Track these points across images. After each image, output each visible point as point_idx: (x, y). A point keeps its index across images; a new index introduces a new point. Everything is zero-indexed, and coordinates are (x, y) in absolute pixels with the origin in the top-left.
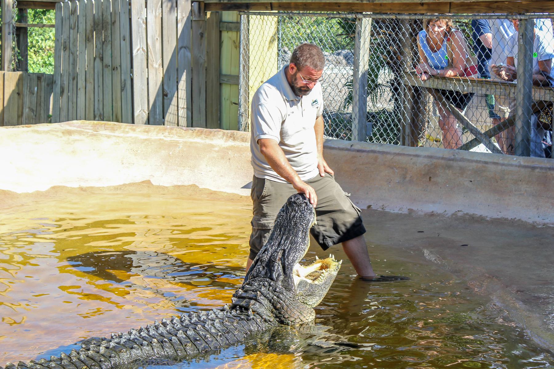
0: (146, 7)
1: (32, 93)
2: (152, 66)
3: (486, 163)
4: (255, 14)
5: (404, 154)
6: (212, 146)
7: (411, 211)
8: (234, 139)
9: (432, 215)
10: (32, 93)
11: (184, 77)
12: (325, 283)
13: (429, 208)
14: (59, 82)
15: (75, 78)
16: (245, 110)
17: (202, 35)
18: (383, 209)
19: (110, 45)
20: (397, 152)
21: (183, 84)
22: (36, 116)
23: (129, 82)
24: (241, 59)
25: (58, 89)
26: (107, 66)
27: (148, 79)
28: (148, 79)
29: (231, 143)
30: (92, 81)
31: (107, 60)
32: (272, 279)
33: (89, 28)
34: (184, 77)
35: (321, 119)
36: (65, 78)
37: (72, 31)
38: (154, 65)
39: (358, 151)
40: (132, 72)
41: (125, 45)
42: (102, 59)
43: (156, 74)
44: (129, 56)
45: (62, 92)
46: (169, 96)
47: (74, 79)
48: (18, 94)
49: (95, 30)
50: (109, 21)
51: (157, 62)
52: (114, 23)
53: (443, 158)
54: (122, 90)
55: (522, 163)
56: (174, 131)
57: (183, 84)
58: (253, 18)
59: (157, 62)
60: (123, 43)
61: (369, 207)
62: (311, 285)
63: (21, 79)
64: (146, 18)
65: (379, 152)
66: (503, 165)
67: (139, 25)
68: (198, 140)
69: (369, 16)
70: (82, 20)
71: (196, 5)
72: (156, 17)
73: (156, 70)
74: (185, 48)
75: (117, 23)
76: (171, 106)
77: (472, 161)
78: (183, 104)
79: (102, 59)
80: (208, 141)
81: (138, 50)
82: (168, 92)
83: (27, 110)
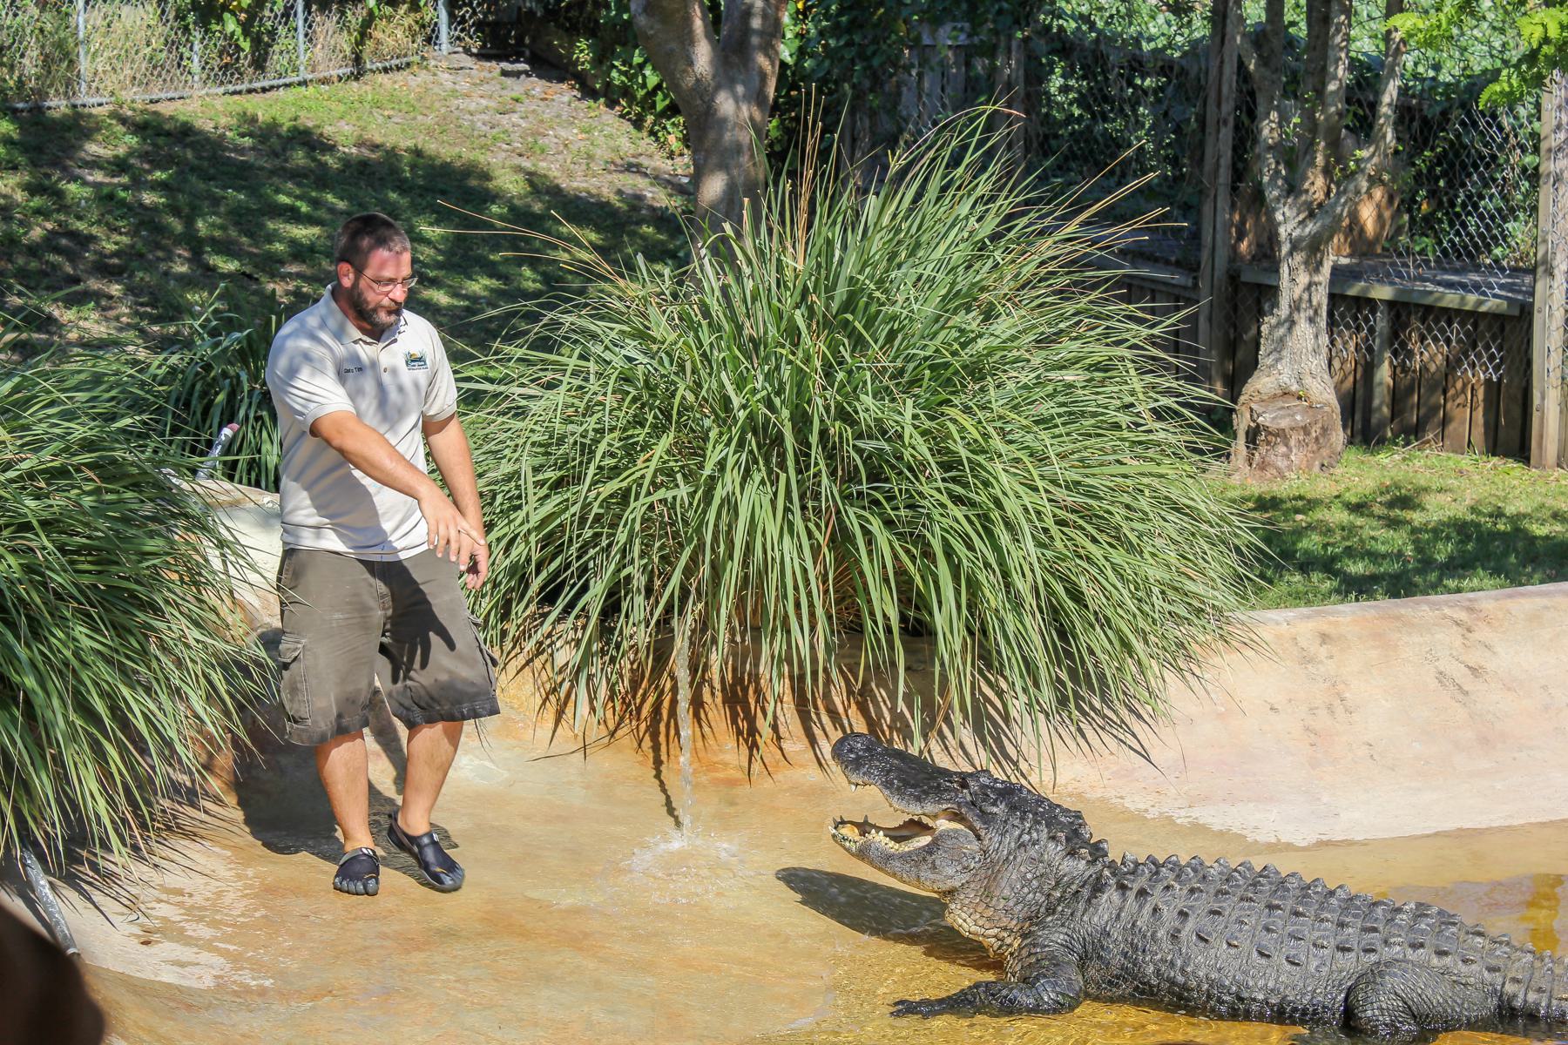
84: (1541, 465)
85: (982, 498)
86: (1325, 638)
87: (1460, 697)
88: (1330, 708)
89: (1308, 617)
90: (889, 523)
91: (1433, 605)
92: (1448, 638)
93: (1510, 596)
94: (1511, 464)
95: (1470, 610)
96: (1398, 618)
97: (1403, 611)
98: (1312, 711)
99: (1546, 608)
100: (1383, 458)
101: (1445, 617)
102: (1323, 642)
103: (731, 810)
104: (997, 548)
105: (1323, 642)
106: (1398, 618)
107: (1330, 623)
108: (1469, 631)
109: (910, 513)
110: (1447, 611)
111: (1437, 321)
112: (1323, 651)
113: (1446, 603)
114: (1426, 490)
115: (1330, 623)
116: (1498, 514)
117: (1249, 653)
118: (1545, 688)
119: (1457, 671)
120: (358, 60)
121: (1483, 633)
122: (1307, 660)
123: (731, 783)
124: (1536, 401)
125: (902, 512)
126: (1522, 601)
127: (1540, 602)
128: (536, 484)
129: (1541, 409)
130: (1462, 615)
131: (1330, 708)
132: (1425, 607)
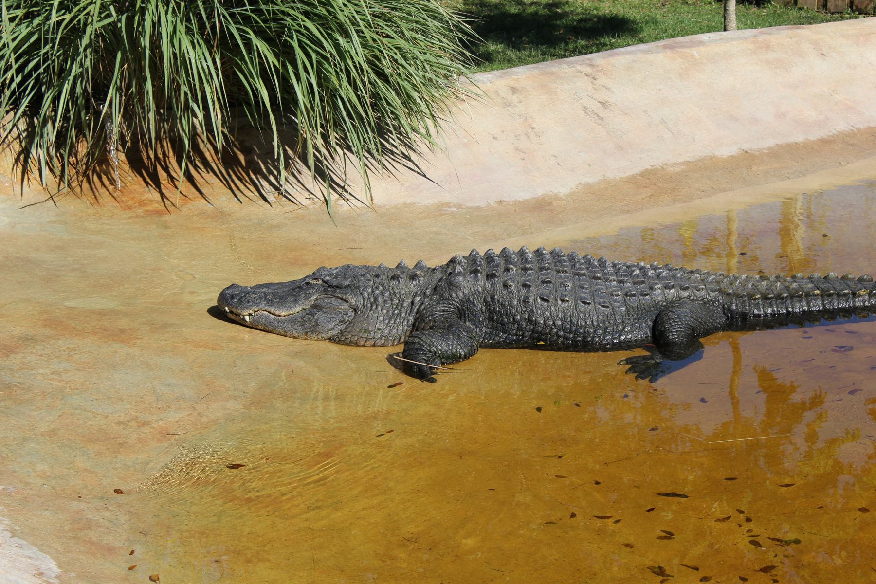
85: (322, 11)
86: (514, 90)
87: (599, 122)
88: (526, 134)
89: (501, 77)
90: (260, 33)
91: (569, 64)
92: (583, 84)
93: (611, 56)
95: (592, 66)
96: (552, 74)
97: (553, 69)
98: (517, 137)
99: (634, 61)
101: (579, 72)
102: (514, 93)
103: (169, 232)
104: (337, 46)
105: (514, 93)
106: (552, 74)
107: (514, 80)
108: (595, 79)
109: (276, 25)
110: (579, 67)
112: (515, 98)
113: (576, 62)
115: (514, 80)
117: (474, 103)
118: (645, 111)
119: (595, 106)
121: (602, 80)
122: (508, 105)
123: (159, 213)
125: (272, 25)
126: (619, 58)
127: (629, 58)
128: (12, 20)
130: (588, 70)
131: (526, 134)
132: (565, 66)
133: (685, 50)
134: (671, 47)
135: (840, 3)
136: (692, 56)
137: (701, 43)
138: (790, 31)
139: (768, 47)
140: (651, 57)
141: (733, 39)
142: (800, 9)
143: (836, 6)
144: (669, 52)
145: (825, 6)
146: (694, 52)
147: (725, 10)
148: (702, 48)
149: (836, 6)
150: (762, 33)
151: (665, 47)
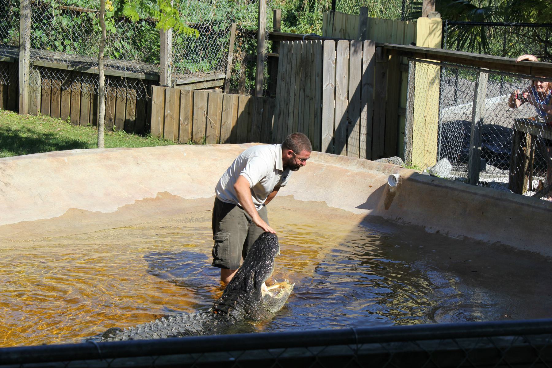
0: (336, 50)
1: (259, 113)
2: (339, 99)
3: (522, 204)
4: (420, 61)
5: (466, 192)
6: (347, 171)
7: (466, 238)
8: (364, 167)
9: (479, 243)
10: (259, 113)
11: (365, 109)
12: (283, 298)
13: (479, 237)
14: (278, 106)
15: (288, 104)
16: (409, 139)
17: (384, 74)
18: (447, 234)
19: (309, 80)
20: (462, 189)
21: (364, 114)
22: (261, 132)
23: (319, 111)
24: (408, 96)
25: (277, 112)
26: (307, 96)
27: (335, 109)
28: (335, 109)
29: (362, 170)
30: (298, 107)
31: (308, 91)
32: (246, 291)
33: (298, 64)
34: (365, 109)
35: (376, 163)
36: (282, 103)
37: (288, 65)
38: (341, 98)
39: (436, 186)
40: (322, 103)
41: (318, 79)
42: (304, 91)
43: (342, 105)
44: (320, 89)
45: (280, 114)
46: (352, 123)
47: (287, 104)
48: (249, 113)
49: (301, 66)
50: (310, 60)
51: (343, 96)
52: (312, 62)
53: (493, 198)
54: (315, 117)
55: (547, 207)
56: (323, 157)
57: (364, 114)
58: (417, 64)
59: (343, 96)
60: (317, 78)
61: (438, 232)
62: (273, 298)
63: (250, 101)
64: (336, 59)
65: (450, 188)
66: (534, 207)
67: (329, 65)
68: (338, 165)
69: (486, 71)
70: (294, 57)
71: (379, 49)
72: (344, 58)
73: (342, 102)
74: (368, 84)
75: (315, 62)
76: (353, 132)
77: (512, 202)
78: (364, 130)
79: (304, 91)
80: (345, 167)
81: (328, 85)
82: (352, 120)
83: (255, 127)
84: (23, 114)
93: (18, 159)
94: (12, 113)
95: (4, 164)
100: (365, 169)
108: (4, 171)
111: (76, 77)
114: (289, 166)
116: (9, 130)
118: (30, 189)
120: (455, 100)
121: (8, 171)
124: (21, 92)
129: (22, 94)
133: (60, 158)
134: (53, 156)
135: (186, 138)
136: (64, 161)
137: (71, 154)
138: (123, 151)
139: (108, 158)
140: (40, 160)
141: (89, 153)
142: (166, 140)
143: (184, 140)
144: (51, 158)
145: (179, 139)
146: (66, 159)
147: (98, 138)
148: (71, 157)
149: (184, 140)
150: (107, 151)
151: (49, 156)
